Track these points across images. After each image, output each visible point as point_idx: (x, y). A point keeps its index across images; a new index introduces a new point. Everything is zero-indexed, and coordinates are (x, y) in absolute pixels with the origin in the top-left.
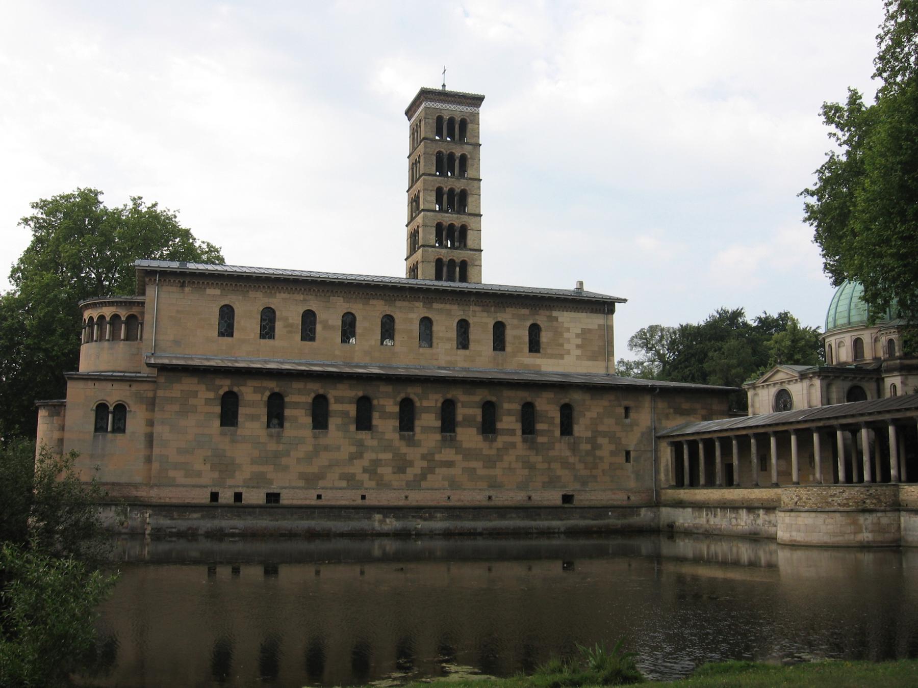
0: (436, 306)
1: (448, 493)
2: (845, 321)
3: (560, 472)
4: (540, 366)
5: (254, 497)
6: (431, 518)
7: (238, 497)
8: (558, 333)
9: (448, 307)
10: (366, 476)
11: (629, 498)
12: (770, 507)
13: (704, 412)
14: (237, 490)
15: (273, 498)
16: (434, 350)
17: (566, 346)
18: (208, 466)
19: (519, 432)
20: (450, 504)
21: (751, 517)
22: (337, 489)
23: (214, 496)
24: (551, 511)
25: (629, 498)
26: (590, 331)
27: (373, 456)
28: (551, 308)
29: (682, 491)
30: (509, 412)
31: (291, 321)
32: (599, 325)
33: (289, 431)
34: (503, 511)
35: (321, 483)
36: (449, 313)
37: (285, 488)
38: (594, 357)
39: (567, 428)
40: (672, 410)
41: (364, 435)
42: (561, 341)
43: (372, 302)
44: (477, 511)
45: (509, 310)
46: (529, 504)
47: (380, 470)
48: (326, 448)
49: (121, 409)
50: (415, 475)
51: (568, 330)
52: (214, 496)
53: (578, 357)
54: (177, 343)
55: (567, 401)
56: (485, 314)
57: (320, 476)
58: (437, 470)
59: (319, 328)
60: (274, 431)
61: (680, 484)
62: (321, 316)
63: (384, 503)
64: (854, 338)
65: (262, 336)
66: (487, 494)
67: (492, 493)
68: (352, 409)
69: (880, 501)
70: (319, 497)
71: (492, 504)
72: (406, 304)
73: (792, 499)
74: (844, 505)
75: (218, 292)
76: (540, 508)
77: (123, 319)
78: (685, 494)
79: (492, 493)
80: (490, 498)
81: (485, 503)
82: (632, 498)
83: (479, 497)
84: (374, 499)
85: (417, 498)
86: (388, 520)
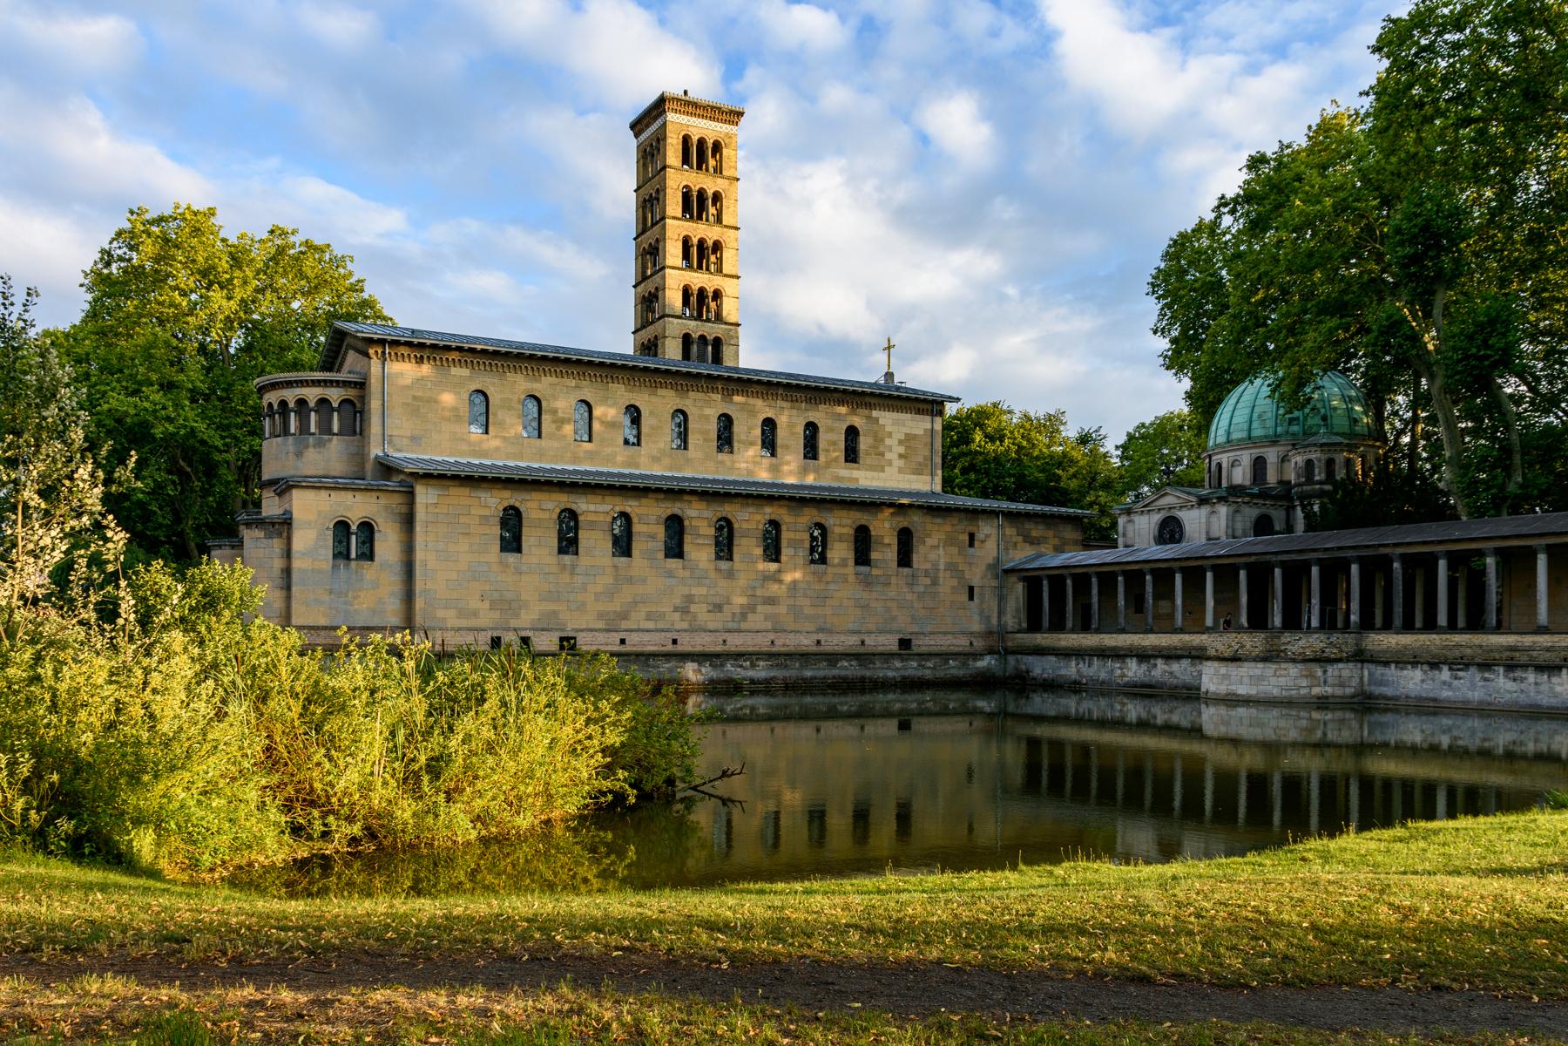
0: (737, 399)
1: (771, 636)
2: (1244, 435)
3: (895, 612)
4: (857, 480)
6: (753, 666)
8: (878, 440)
9: (751, 401)
10: (677, 616)
11: (971, 644)
12: (1198, 655)
13: (1056, 541)
14: (524, 634)
16: (735, 457)
17: (888, 456)
18: (486, 605)
19: (851, 562)
20: (774, 649)
21: (1144, 667)
22: (643, 630)
24: (888, 656)
25: (971, 644)
26: (915, 437)
27: (686, 591)
28: (870, 406)
29: (1039, 636)
30: (841, 539)
31: (560, 414)
32: (925, 430)
33: (584, 560)
34: (832, 658)
35: (624, 625)
36: (753, 413)
37: (582, 630)
38: (918, 472)
39: (905, 559)
40: (1020, 538)
41: (674, 563)
42: (881, 449)
43: (661, 392)
44: (804, 657)
45: (822, 407)
46: (862, 650)
47: (693, 608)
48: (630, 580)
49: (367, 528)
50: (734, 614)
51: (890, 435)
53: (901, 470)
54: (415, 439)
55: (905, 524)
56: (795, 412)
57: (624, 616)
58: (760, 608)
60: (567, 559)
61: (1034, 626)
63: (699, 649)
64: (1254, 456)
66: (815, 637)
67: (821, 636)
68: (660, 531)
69: (1341, 651)
70: (623, 641)
71: (821, 649)
72: (700, 395)
73: (1230, 646)
74: (1300, 654)
75: (465, 372)
76: (874, 655)
77: (335, 405)
78: (1041, 639)
79: (821, 636)
80: (819, 642)
81: (814, 649)
82: (975, 644)
83: (806, 642)
85: (736, 642)
86: (703, 670)
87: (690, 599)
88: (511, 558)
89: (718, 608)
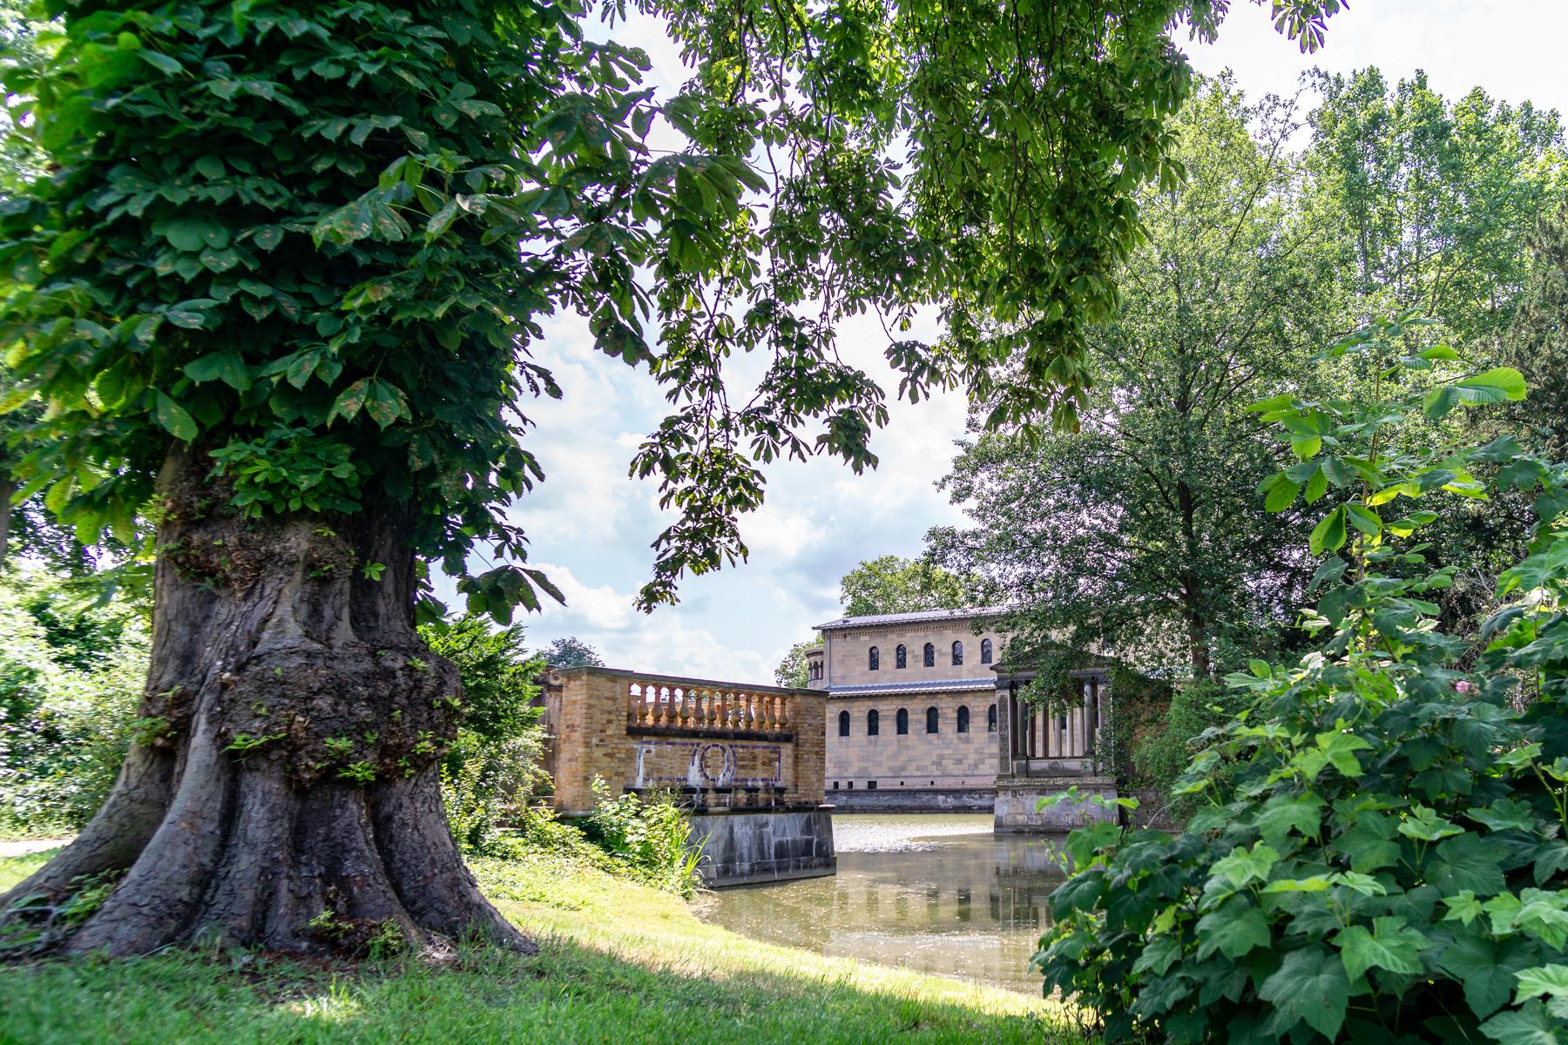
5: (861, 785)
7: (851, 784)
15: (872, 785)
23: (836, 784)
41: (932, 736)
48: (907, 747)
52: (836, 784)
54: (843, 677)
57: (904, 768)
59: (936, 655)
62: (937, 646)
65: (899, 667)
68: (924, 718)
84: (940, 784)
85: (971, 783)
87: (941, 757)
88: (844, 739)
89: (959, 762)
